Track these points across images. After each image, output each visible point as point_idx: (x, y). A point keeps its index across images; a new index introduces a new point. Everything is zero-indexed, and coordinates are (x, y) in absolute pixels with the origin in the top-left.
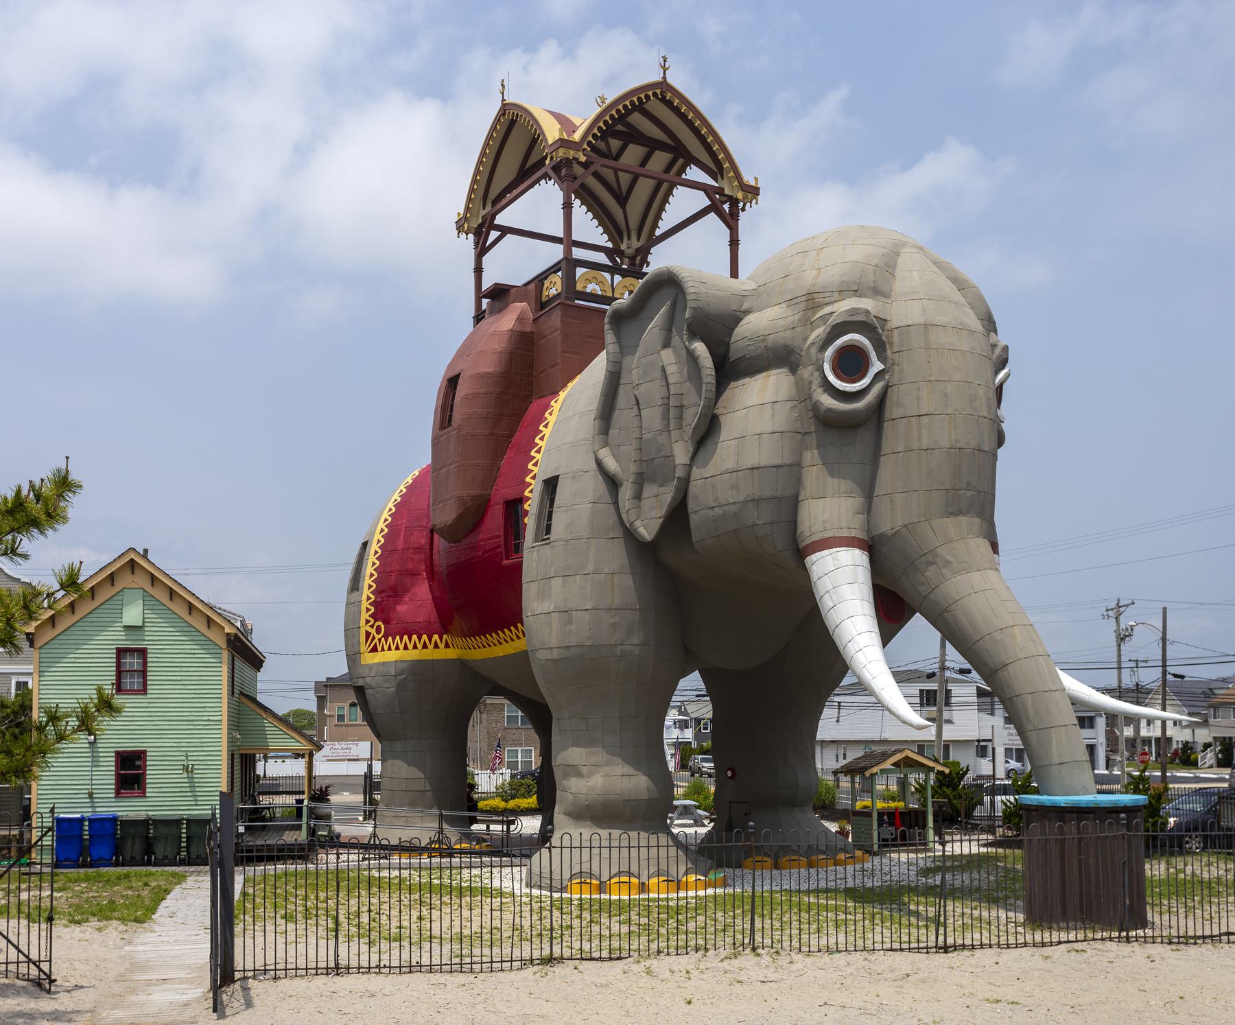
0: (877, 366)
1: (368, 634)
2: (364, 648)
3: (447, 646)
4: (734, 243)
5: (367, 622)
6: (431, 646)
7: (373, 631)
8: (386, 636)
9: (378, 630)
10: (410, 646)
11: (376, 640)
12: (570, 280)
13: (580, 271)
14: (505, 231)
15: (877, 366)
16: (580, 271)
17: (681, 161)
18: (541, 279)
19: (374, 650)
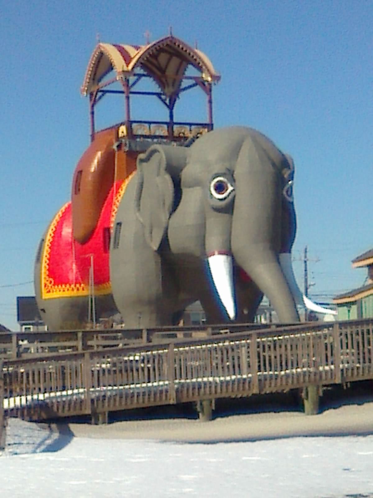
0: (230, 188)
1: (45, 285)
2: (44, 291)
3: (83, 289)
4: (210, 102)
5: (45, 278)
6: (75, 290)
7: (48, 283)
8: (54, 285)
9: (51, 282)
10: (66, 290)
11: (50, 288)
12: (129, 129)
13: (134, 125)
14: (105, 92)
15: (230, 188)
16: (134, 125)
17: (184, 63)
18: (118, 127)
19: (49, 292)
